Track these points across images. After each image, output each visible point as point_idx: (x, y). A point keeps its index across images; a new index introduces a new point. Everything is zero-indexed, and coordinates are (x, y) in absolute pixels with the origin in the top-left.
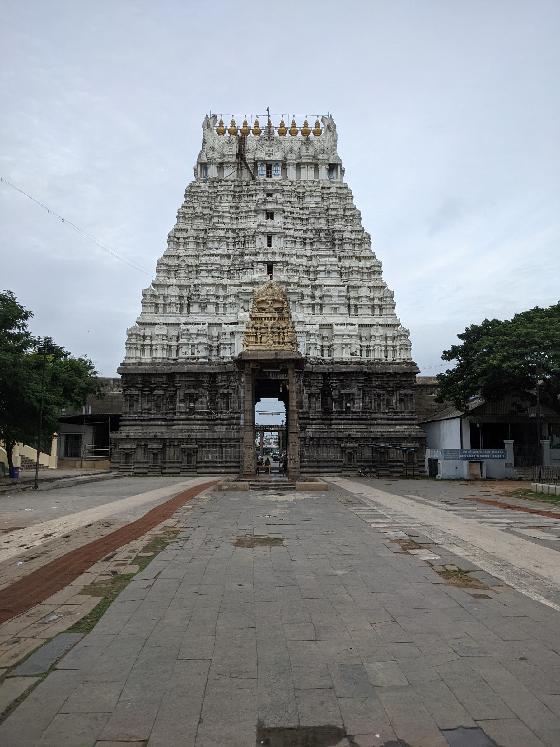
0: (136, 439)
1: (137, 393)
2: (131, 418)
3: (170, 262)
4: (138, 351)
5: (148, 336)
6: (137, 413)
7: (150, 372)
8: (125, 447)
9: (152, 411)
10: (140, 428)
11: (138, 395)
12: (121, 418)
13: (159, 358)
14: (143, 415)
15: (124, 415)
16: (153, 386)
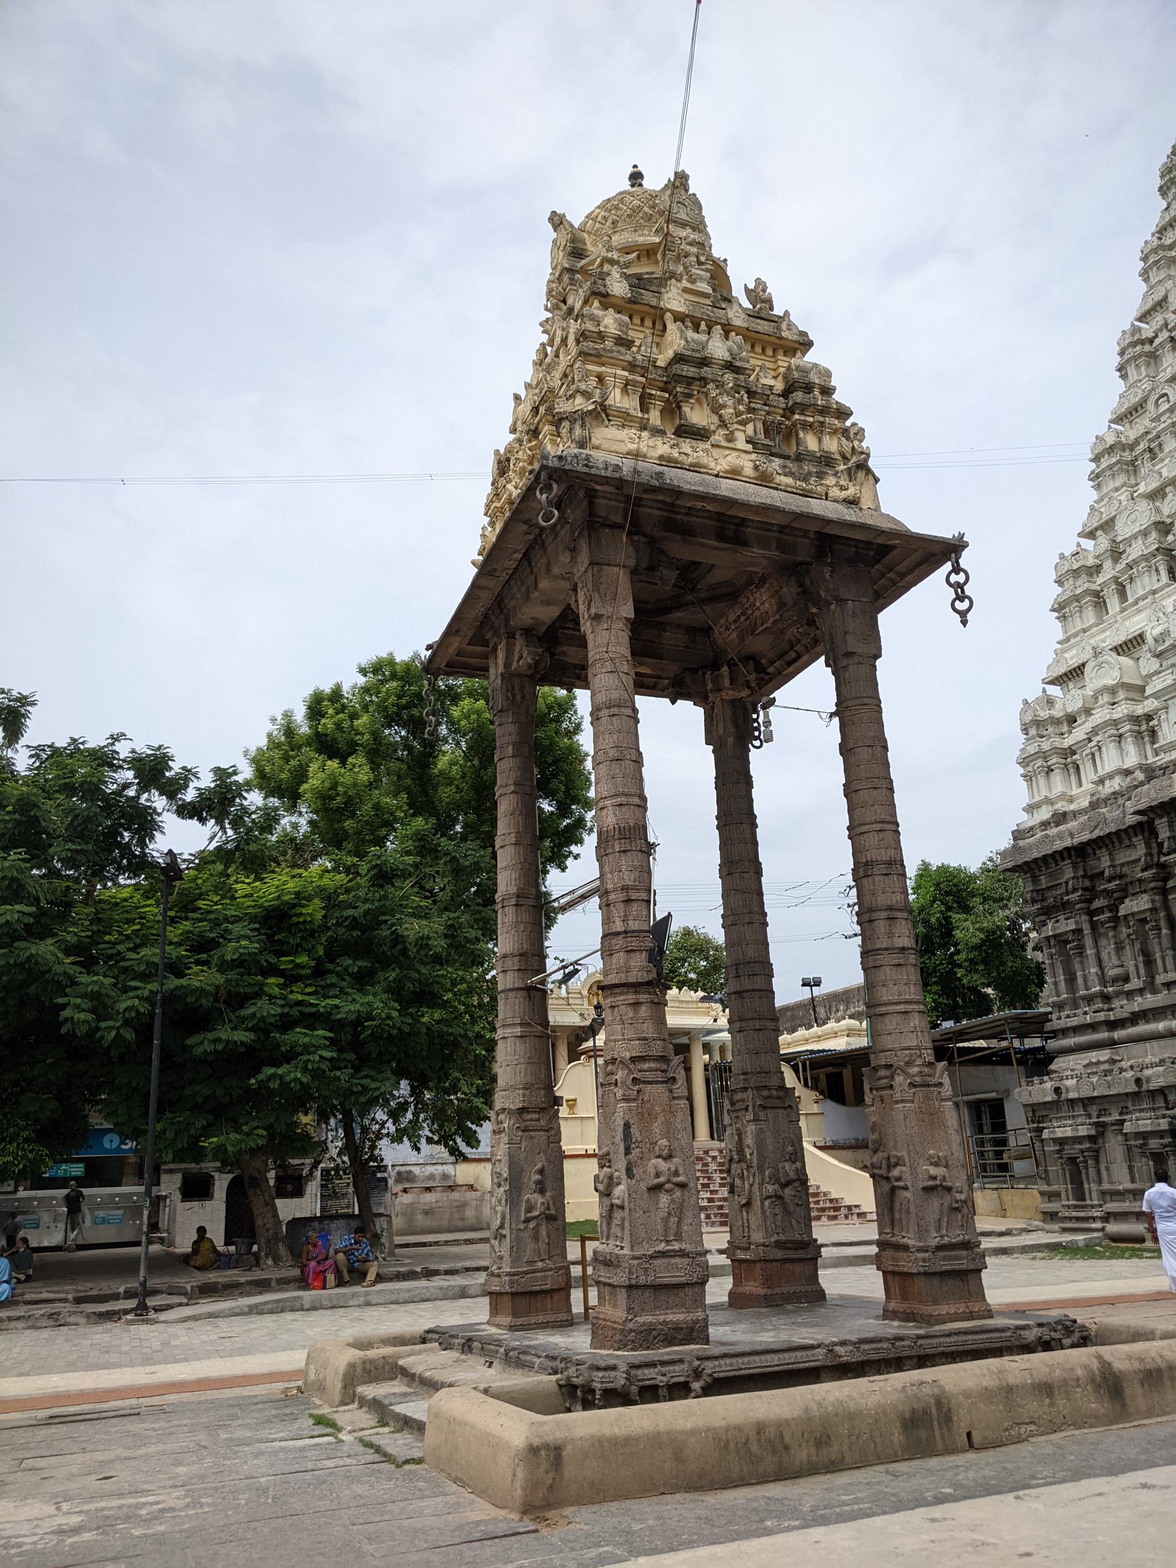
0: (1092, 1100)
1: (1071, 925)
2: (1074, 1022)
3: (1130, 433)
4: (1057, 778)
5: (1079, 712)
6: (1089, 1000)
7: (1085, 837)
8: (1060, 1133)
9: (1135, 983)
10: (1104, 1055)
11: (1078, 931)
12: (1048, 1027)
13: (1111, 776)
14: (1116, 1003)
15: (1054, 1017)
16: (1112, 885)
